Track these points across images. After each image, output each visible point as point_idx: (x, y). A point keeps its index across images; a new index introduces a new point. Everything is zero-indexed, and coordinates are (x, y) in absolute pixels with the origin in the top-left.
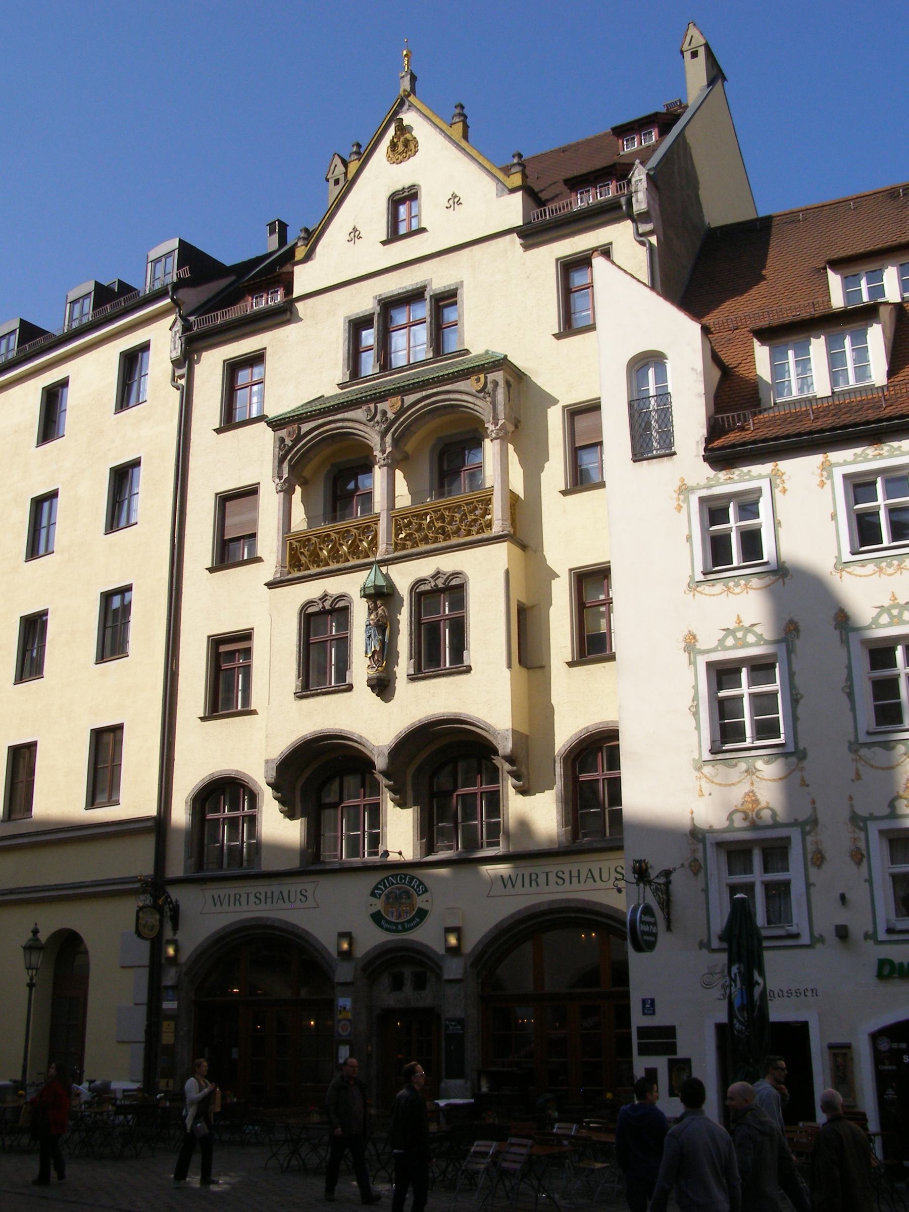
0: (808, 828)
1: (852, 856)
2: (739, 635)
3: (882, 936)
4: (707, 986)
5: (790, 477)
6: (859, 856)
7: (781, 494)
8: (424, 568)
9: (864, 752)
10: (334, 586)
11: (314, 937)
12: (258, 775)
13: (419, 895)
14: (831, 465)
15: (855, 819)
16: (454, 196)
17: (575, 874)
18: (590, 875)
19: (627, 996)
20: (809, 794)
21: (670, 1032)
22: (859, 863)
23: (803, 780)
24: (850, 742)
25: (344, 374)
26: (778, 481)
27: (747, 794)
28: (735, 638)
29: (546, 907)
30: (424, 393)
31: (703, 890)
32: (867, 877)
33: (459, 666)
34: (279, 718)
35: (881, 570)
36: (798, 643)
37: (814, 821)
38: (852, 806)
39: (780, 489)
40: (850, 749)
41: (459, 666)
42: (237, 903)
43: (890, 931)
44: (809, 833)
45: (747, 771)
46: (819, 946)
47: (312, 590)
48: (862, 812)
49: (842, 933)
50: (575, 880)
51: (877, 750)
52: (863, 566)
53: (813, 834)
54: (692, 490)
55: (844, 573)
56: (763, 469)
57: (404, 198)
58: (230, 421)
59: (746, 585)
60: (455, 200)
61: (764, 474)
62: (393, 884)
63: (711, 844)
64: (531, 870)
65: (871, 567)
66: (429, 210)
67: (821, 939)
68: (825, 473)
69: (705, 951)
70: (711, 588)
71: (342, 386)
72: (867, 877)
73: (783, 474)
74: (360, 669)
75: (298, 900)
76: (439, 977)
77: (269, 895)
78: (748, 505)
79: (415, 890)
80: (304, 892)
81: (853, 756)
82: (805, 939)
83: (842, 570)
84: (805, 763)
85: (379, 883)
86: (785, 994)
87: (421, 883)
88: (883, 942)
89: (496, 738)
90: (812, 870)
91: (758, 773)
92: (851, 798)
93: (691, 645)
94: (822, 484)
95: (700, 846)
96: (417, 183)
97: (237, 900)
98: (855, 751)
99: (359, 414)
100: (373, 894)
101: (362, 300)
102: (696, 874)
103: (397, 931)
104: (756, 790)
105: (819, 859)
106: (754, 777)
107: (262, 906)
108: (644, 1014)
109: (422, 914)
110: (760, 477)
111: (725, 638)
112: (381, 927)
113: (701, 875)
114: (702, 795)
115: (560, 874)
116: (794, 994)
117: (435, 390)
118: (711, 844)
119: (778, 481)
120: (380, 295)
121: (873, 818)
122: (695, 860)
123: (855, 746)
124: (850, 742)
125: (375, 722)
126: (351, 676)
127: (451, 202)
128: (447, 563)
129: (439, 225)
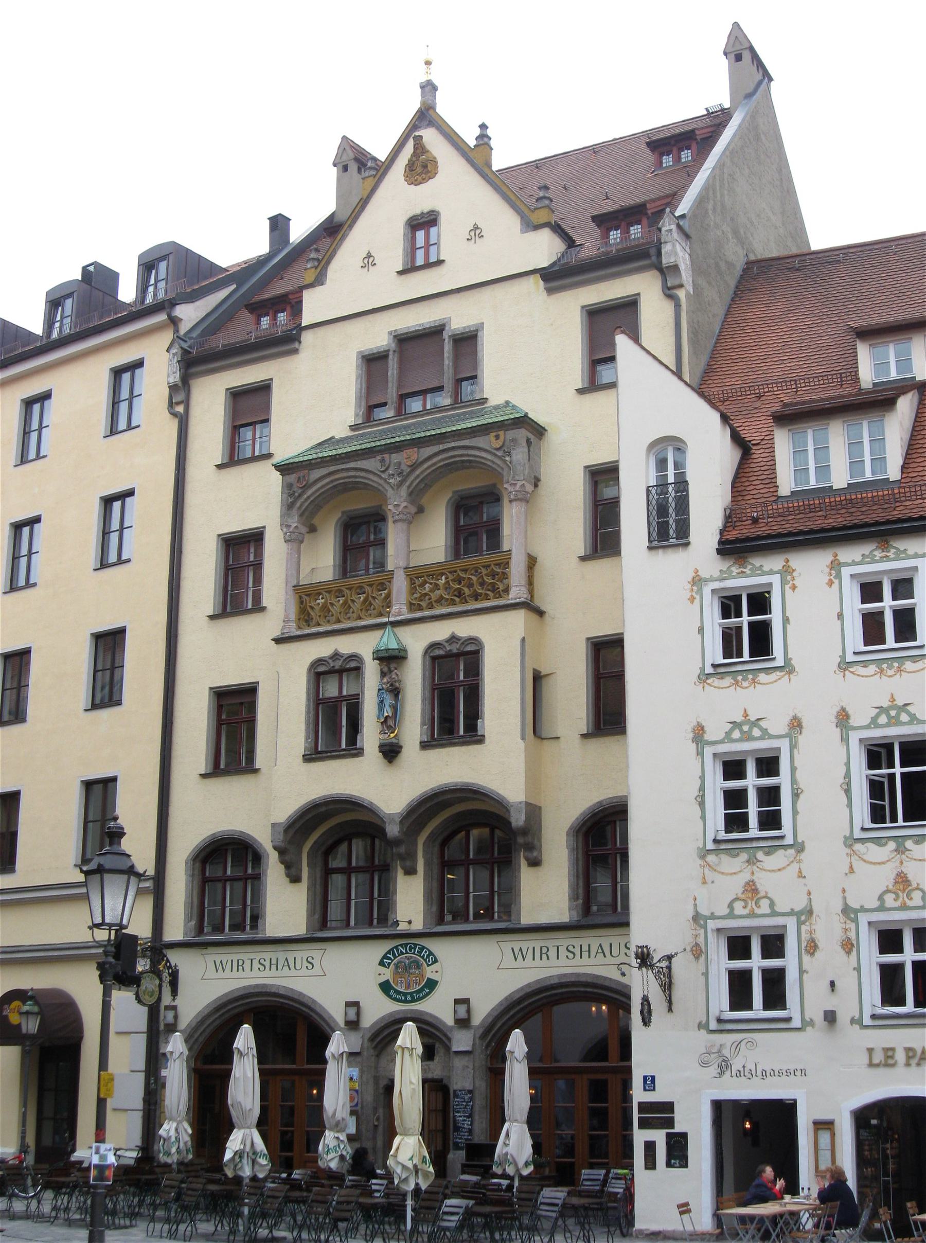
0: (803, 918)
1: (842, 946)
2: (746, 728)
3: (867, 1021)
4: (704, 1064)
5: (800, 574)
6: (849, 946)
7: (790, 591)
8: (440, 632)
9: (858, 847)
10: (346, 645)
11: (320, 1006)
12: (264, 838)
13: (428, 965)
14: (840, 565)
15: (847, 910)
16: (476, 228)
17: (585, 948)
18: (600, 950)
19: (629, 1070)
20: (805, 885)
21: (668, 1107)
22: (848, 953)
23: (800, 872)
24: (845, 837)
25: (356, 415)
26: (789, 578)
27: (747, 883)
28: (742, 732)
29: (556, 981)
30: (442, 447)
31: (703, 974)
32: (856, 966)
33: (473, 735)
34: (286, 781)
35: (882, 671)
36: (801, 739)
37: (810, 912)
38: (845, 898)
39: (790, 585)
40: (845, 843)
41: (473, 735)
42: (240, 968)
43: (874, 1017)
44: (804, 923)
45: (748, 861)
46: (809, 1029)
47: (323, 648)
48: (854, 904)
49: (830, 1017)
50: (585, 954)
51: (870, 845)
52: (865, 666)
53: (807, 924)
54: (706, 581)
55: (847, 672)
56: (774, 562)
57: (423, 223)
58: (234, 458)
59: (753, 680)
60: (476, 232)
61: (775, 569)
62: (402, 953)
63: (712, 930)
64: (542, 943)
65: (872, 668)
66: (449, 238)
67: (812, 1023)
68: (833, 572)
69: (703, 1032)
70: (721, 681)
71: (353, 428)
72: (856, 966)
73: (794, 570)
74: (371, 735)
75: (304, 967)
76: (448, 1048)
77: (274, 962)
78: (760, 602)
79: (425, 960)
80: (310, 959)
81: (848, 851)
82: (796, 1023)
83: (845, 669)
84: (803, 856)
85: (388, 952)
86: (777, 1073)
87: (431, 953)
88: (867, 1027)
89: (508, 811)
90: (806, 958)
91: (758, 864)
92: (844, 891)
93: (699, 735)
94: (830, 583)
95: (702, 931)
96: (437, 209)
97: (240, 965)
98: (850, 846)
99: (372, 464)
100: (381, 963)
101: (377, 336)
102: (697, 958)
103: (406, 1001)
104: (756, 880)
105: (812, 947)
106: (755, 867)
107: (267, 973)
108: (645, 1090)
109: (432, 985)
110: (771, 572)
111: (732, 730)
112: (390, 997)
113: (702, 959)
114: (705, 883)
115: (570, 948)
116: (785, 1073)
117: (453, 444)
118: (712, 930)
119: (789, 578)
120: (395, 331)
121: (863, 909)
122: (697, 945)
123: (850, 841)
124: (845, 837)
125: (388, 788)
126: (362, 740)
127: (472, 233)
128: (464, 628)
129: (461, 261)
